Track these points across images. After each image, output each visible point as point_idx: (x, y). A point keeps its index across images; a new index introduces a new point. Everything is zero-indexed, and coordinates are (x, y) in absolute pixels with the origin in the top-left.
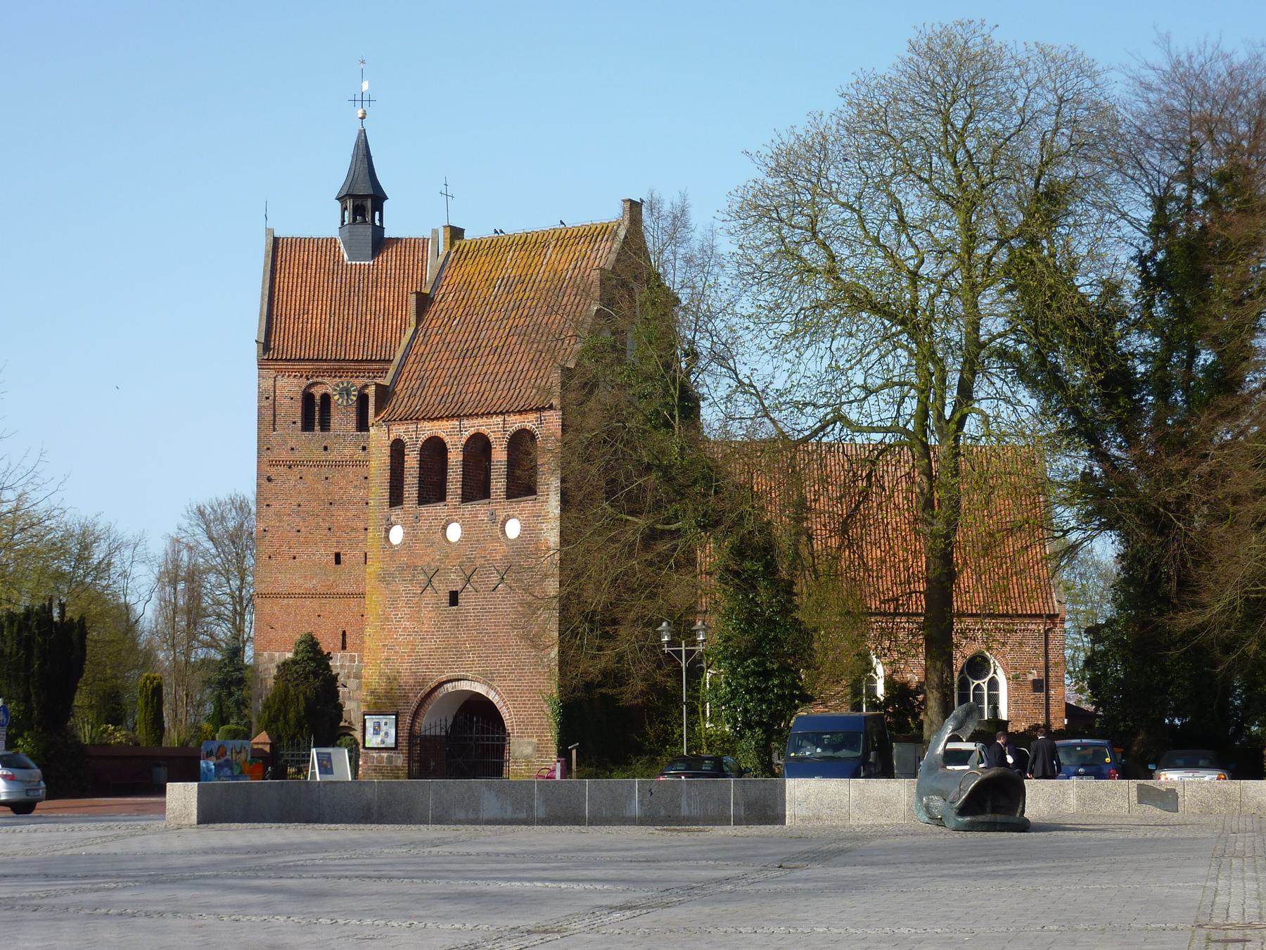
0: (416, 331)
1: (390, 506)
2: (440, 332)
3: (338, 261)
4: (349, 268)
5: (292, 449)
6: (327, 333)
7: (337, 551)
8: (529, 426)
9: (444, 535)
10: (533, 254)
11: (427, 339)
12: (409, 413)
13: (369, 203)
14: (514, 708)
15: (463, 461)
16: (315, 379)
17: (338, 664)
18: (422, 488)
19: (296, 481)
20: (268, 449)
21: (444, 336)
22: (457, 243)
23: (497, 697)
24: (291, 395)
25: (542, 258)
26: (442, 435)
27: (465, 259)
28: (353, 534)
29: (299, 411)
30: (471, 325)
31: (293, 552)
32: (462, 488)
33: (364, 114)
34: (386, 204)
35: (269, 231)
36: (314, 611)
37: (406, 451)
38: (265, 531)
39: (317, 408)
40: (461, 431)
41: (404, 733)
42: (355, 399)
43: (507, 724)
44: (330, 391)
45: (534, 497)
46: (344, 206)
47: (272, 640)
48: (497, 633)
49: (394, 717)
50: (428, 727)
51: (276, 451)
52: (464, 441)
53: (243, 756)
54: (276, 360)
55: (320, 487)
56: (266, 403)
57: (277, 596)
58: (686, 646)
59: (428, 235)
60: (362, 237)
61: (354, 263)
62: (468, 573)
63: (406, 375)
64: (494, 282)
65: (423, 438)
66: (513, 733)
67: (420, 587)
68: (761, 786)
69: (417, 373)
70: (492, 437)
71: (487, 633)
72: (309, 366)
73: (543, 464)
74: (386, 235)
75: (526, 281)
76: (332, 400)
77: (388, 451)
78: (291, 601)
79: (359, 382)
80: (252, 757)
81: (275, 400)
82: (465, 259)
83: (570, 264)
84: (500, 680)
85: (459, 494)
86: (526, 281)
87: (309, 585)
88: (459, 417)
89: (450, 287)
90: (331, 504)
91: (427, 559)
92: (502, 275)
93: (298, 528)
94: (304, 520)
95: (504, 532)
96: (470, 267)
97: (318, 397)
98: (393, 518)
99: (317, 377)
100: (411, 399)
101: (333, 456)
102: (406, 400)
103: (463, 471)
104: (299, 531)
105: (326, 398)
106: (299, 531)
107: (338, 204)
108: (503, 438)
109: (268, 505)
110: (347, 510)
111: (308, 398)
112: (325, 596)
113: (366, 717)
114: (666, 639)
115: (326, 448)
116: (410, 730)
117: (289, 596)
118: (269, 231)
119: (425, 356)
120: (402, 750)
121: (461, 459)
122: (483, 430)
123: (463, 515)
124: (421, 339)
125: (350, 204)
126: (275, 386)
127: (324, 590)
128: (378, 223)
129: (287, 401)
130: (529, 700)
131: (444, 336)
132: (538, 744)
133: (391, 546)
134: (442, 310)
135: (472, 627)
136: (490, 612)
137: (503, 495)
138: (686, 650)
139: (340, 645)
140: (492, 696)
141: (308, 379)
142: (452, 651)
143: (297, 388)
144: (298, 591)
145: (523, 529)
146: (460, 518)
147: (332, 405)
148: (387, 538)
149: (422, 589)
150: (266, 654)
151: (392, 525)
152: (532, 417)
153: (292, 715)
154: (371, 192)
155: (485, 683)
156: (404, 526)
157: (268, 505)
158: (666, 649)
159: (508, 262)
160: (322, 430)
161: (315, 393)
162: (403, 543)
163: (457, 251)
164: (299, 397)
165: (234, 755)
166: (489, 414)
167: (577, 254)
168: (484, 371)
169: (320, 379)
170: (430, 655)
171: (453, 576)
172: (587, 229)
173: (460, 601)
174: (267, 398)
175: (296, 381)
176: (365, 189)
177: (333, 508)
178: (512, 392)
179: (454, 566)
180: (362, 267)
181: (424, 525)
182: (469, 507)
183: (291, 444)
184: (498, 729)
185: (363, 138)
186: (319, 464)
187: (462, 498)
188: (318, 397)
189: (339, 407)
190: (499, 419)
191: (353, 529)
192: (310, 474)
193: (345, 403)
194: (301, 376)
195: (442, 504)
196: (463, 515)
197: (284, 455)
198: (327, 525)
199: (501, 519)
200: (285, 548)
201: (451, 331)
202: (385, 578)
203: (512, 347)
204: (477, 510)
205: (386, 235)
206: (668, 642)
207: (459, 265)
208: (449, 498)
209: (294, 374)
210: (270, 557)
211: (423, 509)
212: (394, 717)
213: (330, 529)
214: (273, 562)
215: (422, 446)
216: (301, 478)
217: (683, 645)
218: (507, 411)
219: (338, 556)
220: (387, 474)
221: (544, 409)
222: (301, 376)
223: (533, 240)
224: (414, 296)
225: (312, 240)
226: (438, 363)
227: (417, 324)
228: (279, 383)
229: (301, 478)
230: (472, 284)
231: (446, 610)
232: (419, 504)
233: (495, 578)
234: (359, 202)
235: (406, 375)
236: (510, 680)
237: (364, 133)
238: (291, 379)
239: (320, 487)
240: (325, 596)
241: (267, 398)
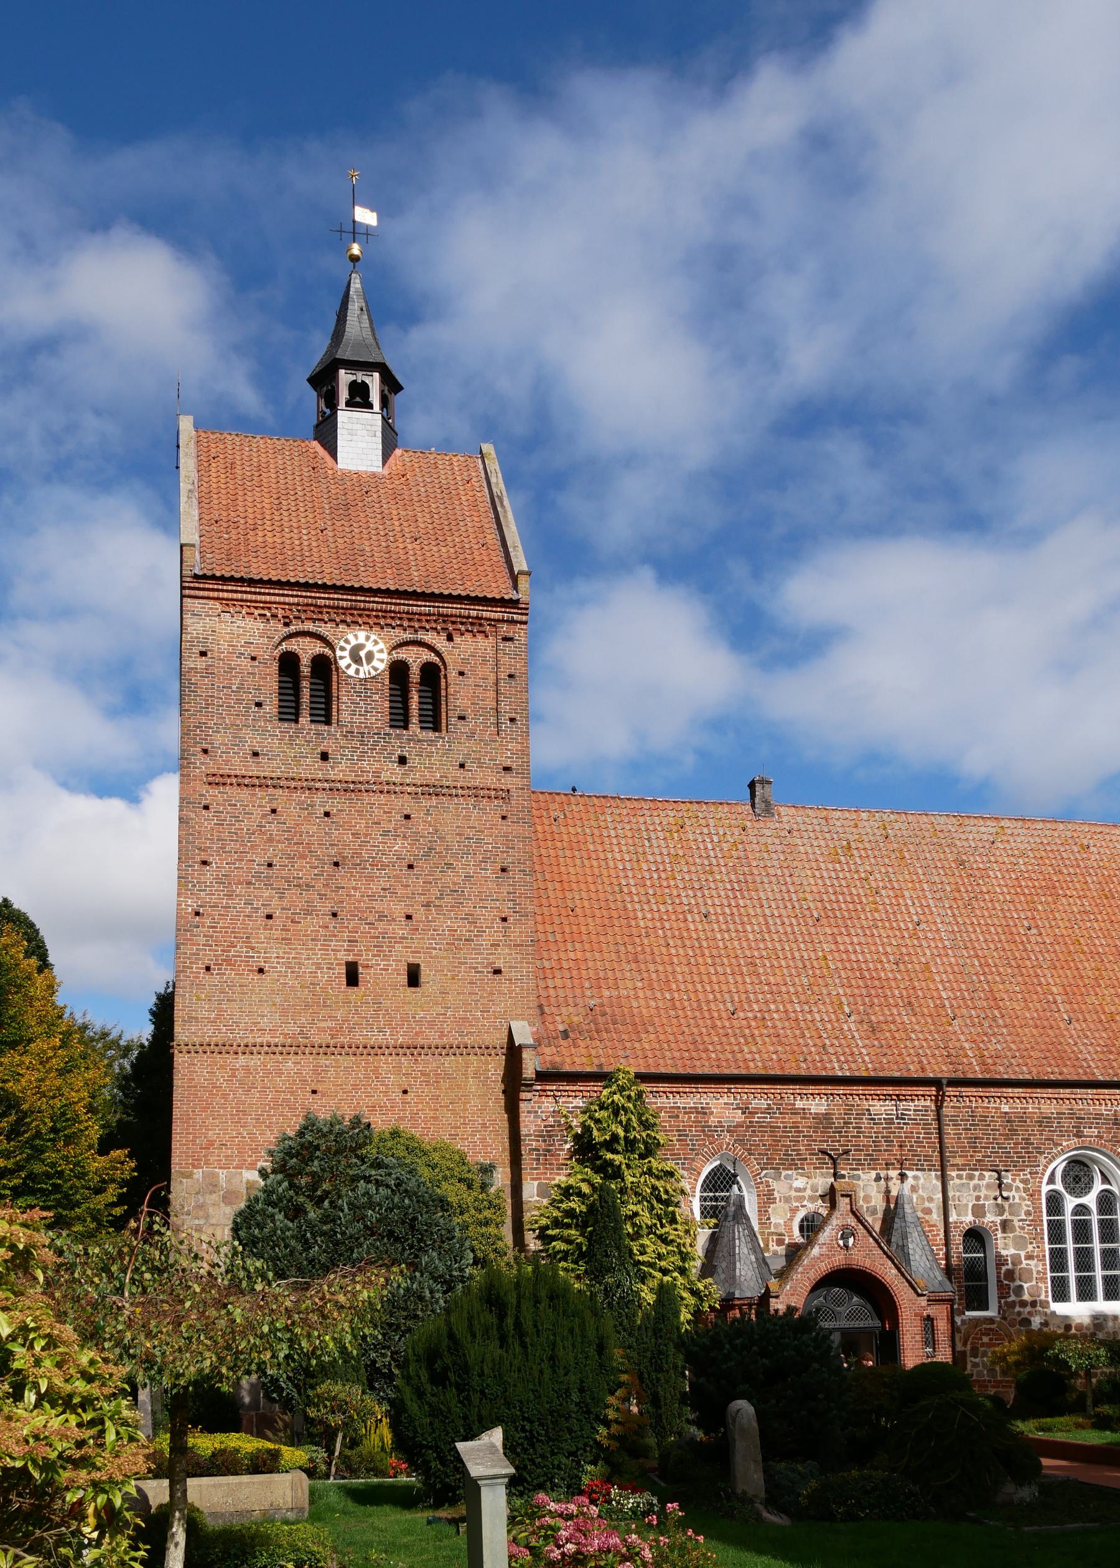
5: (256, 754)
7: (350, 958)
19: (264, 816)
20: (205, 751)
28: (381, 926)
38: (197, 914)
57: (223, 1048)
72: (292, 598)
78: (255, 1061)
87: (292, 1028)
90: (336, 864)
93: (268, 911)
101: (339, 771)
104: (269, 917)
106: (269, 917)
109: (205, 863)
110: (370, 878)
111: (288, 663)
112: (326, 1049)
115: (325, 756)
117: (248, 1049)
127: (326, 1039)
129: (245, 663)
144: (266, 1039)
150: (198, 1174)
157: (205, 863)
161: (300, 653)
164: (270, 656)
169: (309, 626)
183: (252, 741)
191: (382, 917)
192: (290, 805)
197: (239, 765)
198: (328, 906)
210: (208, 969)
214: (214, 978)
216: (274, 811)
229: (274, 811)
238: (249, 623)
239: (313, 828)
240: (326, 1049)
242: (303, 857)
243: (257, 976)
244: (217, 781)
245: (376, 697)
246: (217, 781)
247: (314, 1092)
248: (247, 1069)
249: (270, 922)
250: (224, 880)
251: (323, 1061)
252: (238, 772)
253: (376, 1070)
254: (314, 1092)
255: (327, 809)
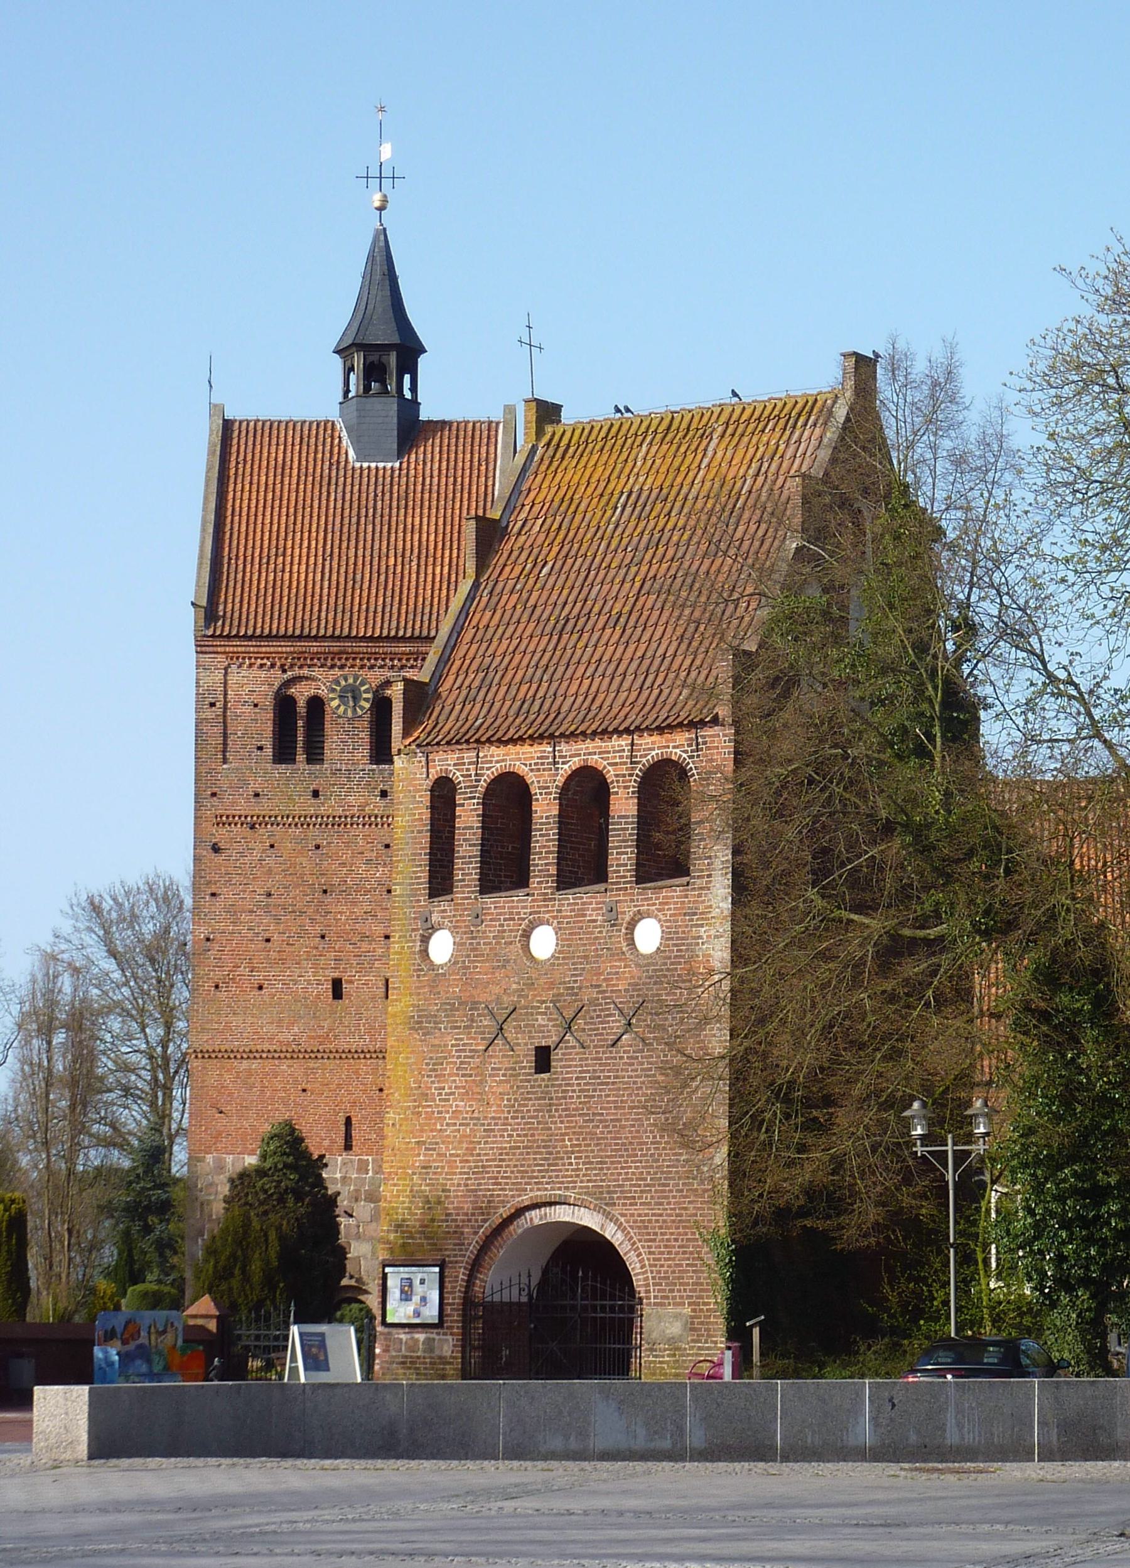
0: (476, 585)
1: (431, 895)
2: (518, 587)
3: (337, 462)
4: (357, 475)
5: (257, 795)
6: (318, 590)
7: (336, 975)
8: (676, 754)
9: (526, 948)
10: (682, 449)
11: (495, 599)
12: (463, 730)
13: (392, 359)
14: (650, 1253)
15: (560, 816)
16: (297, 672)
17: (338, 1175)
18: (489, 863)
19: (264, 851)
21: (525, 595)
22: (549, 429)
23: (619, 1235)
24: (255, 698)
25: (699, 456)
26: (522, 770)
27: (563, 458)
28: (365, 946)
29: (269, 727)
30: (573, 576)
31: (259, 976)
32: (558, 864)
33: (385, 200)
34: (422, 361)
35: (216, 409)
36: (296, 1081)
37: (459, 799)
38: (208, 939)
39: (300, 723)
40: (555, 763)
41: (455, 1299)
42: (367, 705)
43: (638, 1282)
44: (323, 692)
45: (685, 880)
46: (349, 364)
47: (220, 1133)
48: (619, 1120)
49: (437, 1269)
50: (497, 1288)
51: (228, 799)
52: (560, 780)
53: (169, 1338)
54: (228, 637)
55: (304, 861)
56: (209, 713)
57: (230, 1055)
58: (955, 1144)
59: (497, 415)
60: (380, 420)
61: (365, 465)
62: (569, 1014)
63: (458, 663)
64: (614, 500)
65: (488, 775)
66: (648, 1298)
67: (483, 1039)
68: (1089, 1393)
69: (478, 661)
70: (611, 774)
71: (601, 1121)
72: (286, 647)
73: (701, 822)
74: (424, 416)
75: (671, 498)
76: (327, 709)
77: (425, 798)
78: (255, 1065)
79: (376, 677)
80: (185, 1341)
81: (225, 708)
82: (563, 458)
83: (749, 467)
84: (624, 1204)
85: (552, 875)
86: (671, 498)
87: (286, 1036)
88: (552, 738)
89: (537, 508)
90: (325, 892)
91: (496, 990)
92: (629, 486)
93: (267, 935)
94: (278, 920)
95: (631, 943)
96: (571, 473)
97: (301, 703)
98: (435, 918)
99: (301, 667)
100: (468, 707)
101: (329, 806)
102: (458, 707)
103: (559, 834)
104: (268, 940)
105: (316, 704)
106: (268, 940)
107: (338, 361)
108: (631, 775)
109: (213, 895)
110: (354, 903)
111: (284, 705)
112: (314, 1055)
113: (387, 1270)
114: (919, 1131)
115: (316, 794)
116: (466, 1292)
117: (251, 1055)
118: (216, 409)
119: (491, 630)
120: (452, 1328)
121: (557, 813)
122: (595, 760)
123: (560, 911)
124: (485, 599)
125: (358, 360)
126: (225, 683)
128: (408, 394)
129: (248, 709)
130: (676, 1240)
131: (525, 595)
132: (692, 1317)
133: (433, 966)
134: (522, 549)
135: (576, 1109)
136: (607, 1084)
137: (630, 876)
138: (954, 1151)
139: (341, 1141)
140: (611, 1233)
141: (284, 671)
142: (541, 1153)
143: (264, 688)
144: (266, 1047)
145: (666, 937)
146: (554, 917)
147: (327, 718)
148: (425, 953)
149: (487, 1042)
150: (209, 1158)
151: (434, 929)
152: (682, 737)
153: (256, 1267)
154: (395, 339)
155: (598, 1209)
156: (454, 930)
157: (213, 895)
158: (919, 1149)
159: (639, 464)
160: (309, 761)
161: (297, 695)
162: (454, 962)
163: (548, 444)
164: (269, 702)
165: (153, 1337)
166: (605, 733)
167: (761, 449)
168: (596, 657)
169: (305, 672)
170: (501, 1160)
171: (541, 1020)
172: (780, 405)
173: (553, 1064)
174: (212, 705)
175: (263, 674)
176: (386, 334)
177: (328, 899)
178: (645, 693)
179: (544, 1002)
180: (381, 472)
181: (490, 930)
182: (569, 897)
184: (622, 1290)
185: (382, 244)
186: (304, 822)
187: (558, 882)
188: (301, 703)
189: (340, 721)
190: (624, 742)
191: (364, 937)
193: (350, 714)
194: (273, 666)
195: (521, 892)
196: (560, 911)
197: (243, 806)
199: (627, 918)
200: (244, 970)
201: (538, 585)
202: (421, 1023)
203: (646, 613)
204: (584, 904)
205: (424, 416)
206: (923, 1138)
207: (553, 468)
208: (534, 882)
209: (259, 661)
210: (217, 987)
211: (489, 901)
212: (437, 1269)
213: (323, 937)
214: (222, 995)
215: (487, 788)
216: (272, 846)
217: (950, 1142)
218: (638, 728)
219: (337, 985)
220: (425, 840)
221: (702, 724)
222: (273, 666)
223: (684, 425)
224: (473, 523)
225: (291, 425)
226: (515, 642)
227: (479, 573)
228: (233, 679)
229: (272, 846)
230: (576, 502)
231: (529, 1080)
232: (481, 892)
233: (616, 1023)
234: (374, 357)
235: (458, 663)
236: (641, 1204)
237: (382, 235)
238: (255, 671)
240: (314, 1055)
241: (212, 705)
242: (297, 886)
243: (257, 993)
244: (222, 821)
245: (362, 735)
246: (222, 821)
247: (304, 1090)
248: (249, 1072)
249: (269, 945)
250: (232, 911)
251: (312, 1064)
252: (243, 813)
253: (356, 1072)
254: (304, 1090)
255: (318, 842)
